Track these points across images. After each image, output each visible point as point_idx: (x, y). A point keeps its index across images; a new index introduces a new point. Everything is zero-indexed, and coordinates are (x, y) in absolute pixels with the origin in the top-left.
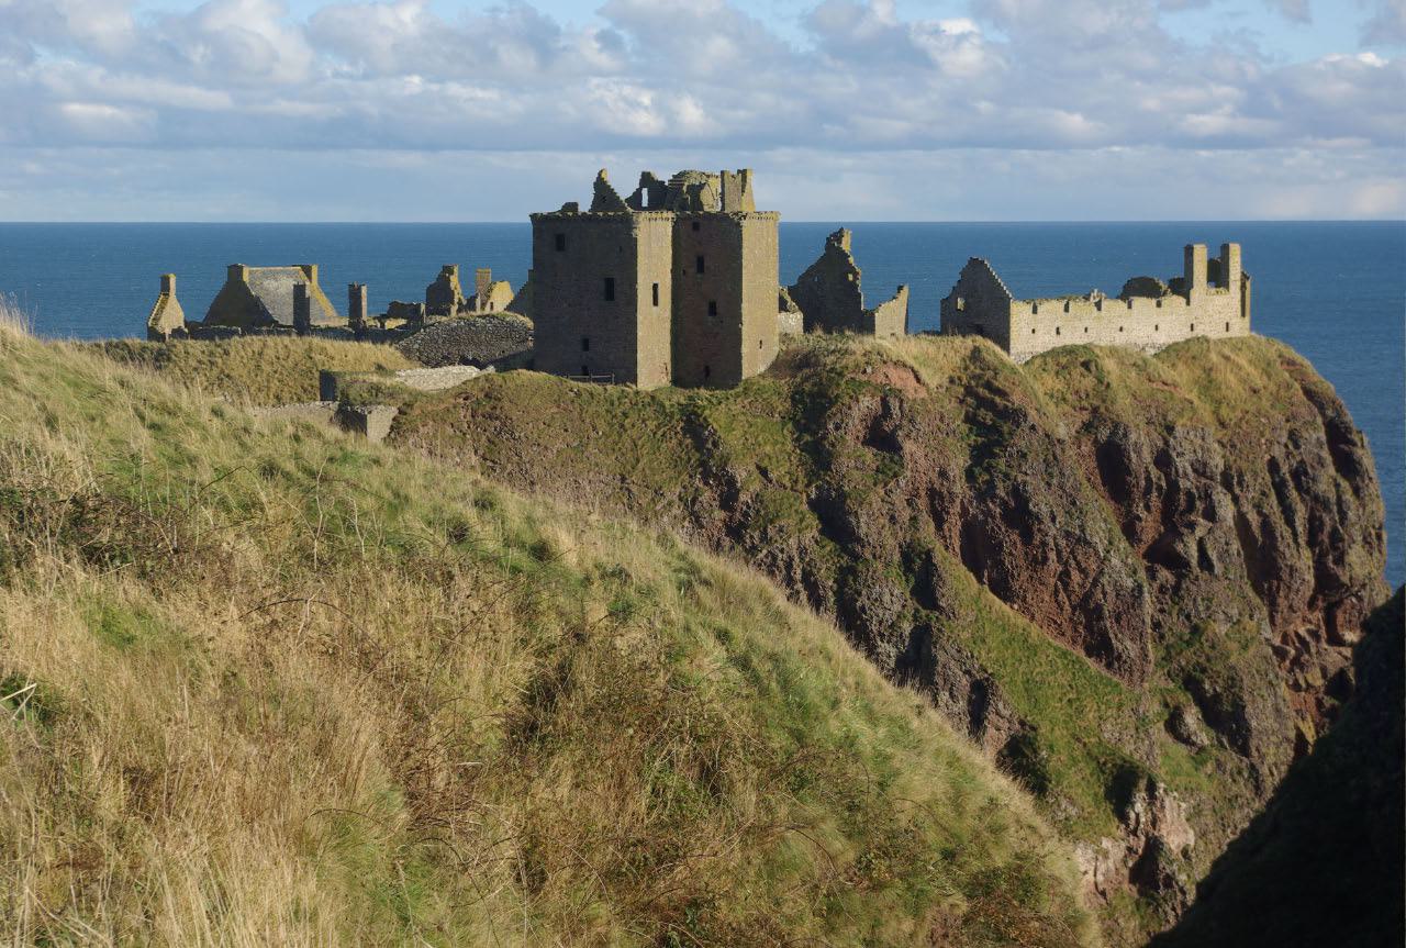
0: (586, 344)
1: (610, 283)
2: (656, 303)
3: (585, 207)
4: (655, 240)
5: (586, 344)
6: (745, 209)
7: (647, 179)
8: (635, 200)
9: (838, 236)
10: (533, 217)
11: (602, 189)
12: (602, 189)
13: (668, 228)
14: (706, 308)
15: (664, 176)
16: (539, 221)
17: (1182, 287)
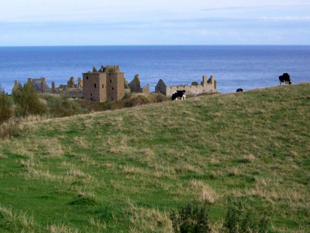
0: (91, 95)
1: (95, 85)
2: (103, 87)
3: (91, 71)
4: (103, 79)
5: (91, 95)
6: (118, 72)
7: (102, 67)
8: (100, 71)
9: (137, 75)
10: (83, 74)
11: (94, 70)
12: (94, 70)
13: (105, 75)
14: (111, 88)
15: (105, 66)
16: (84, 75)
17: (202, 84)
